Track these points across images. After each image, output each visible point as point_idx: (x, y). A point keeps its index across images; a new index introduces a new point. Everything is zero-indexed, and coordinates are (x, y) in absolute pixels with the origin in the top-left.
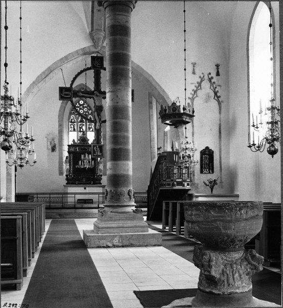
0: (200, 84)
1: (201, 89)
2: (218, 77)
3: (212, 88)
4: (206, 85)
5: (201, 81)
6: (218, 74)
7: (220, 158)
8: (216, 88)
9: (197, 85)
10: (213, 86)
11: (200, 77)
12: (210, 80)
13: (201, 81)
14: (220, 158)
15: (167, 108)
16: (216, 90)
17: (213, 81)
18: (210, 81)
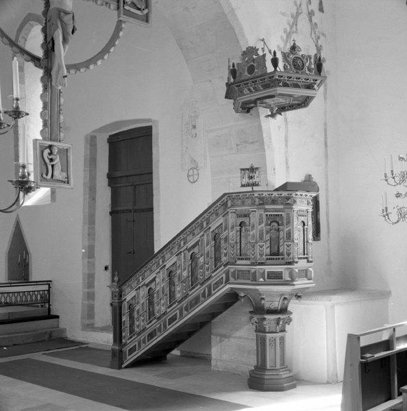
0: (296, 17)
1: (296, 32)
2: (321, 13)
3: (313, 35)
4: (303, 22)
5: (298, 14)
6: (321, 10)
7: (327, 204)
8: (319, 38)
9: (291, 20)
10: (315, 33)
11: (296, 5)
12: (311, 14)
13: (298, 14)
14: (327, 204)
15: (279, 56)
16: (320, 43)
17: (314, 20)
18: (311, 20)
